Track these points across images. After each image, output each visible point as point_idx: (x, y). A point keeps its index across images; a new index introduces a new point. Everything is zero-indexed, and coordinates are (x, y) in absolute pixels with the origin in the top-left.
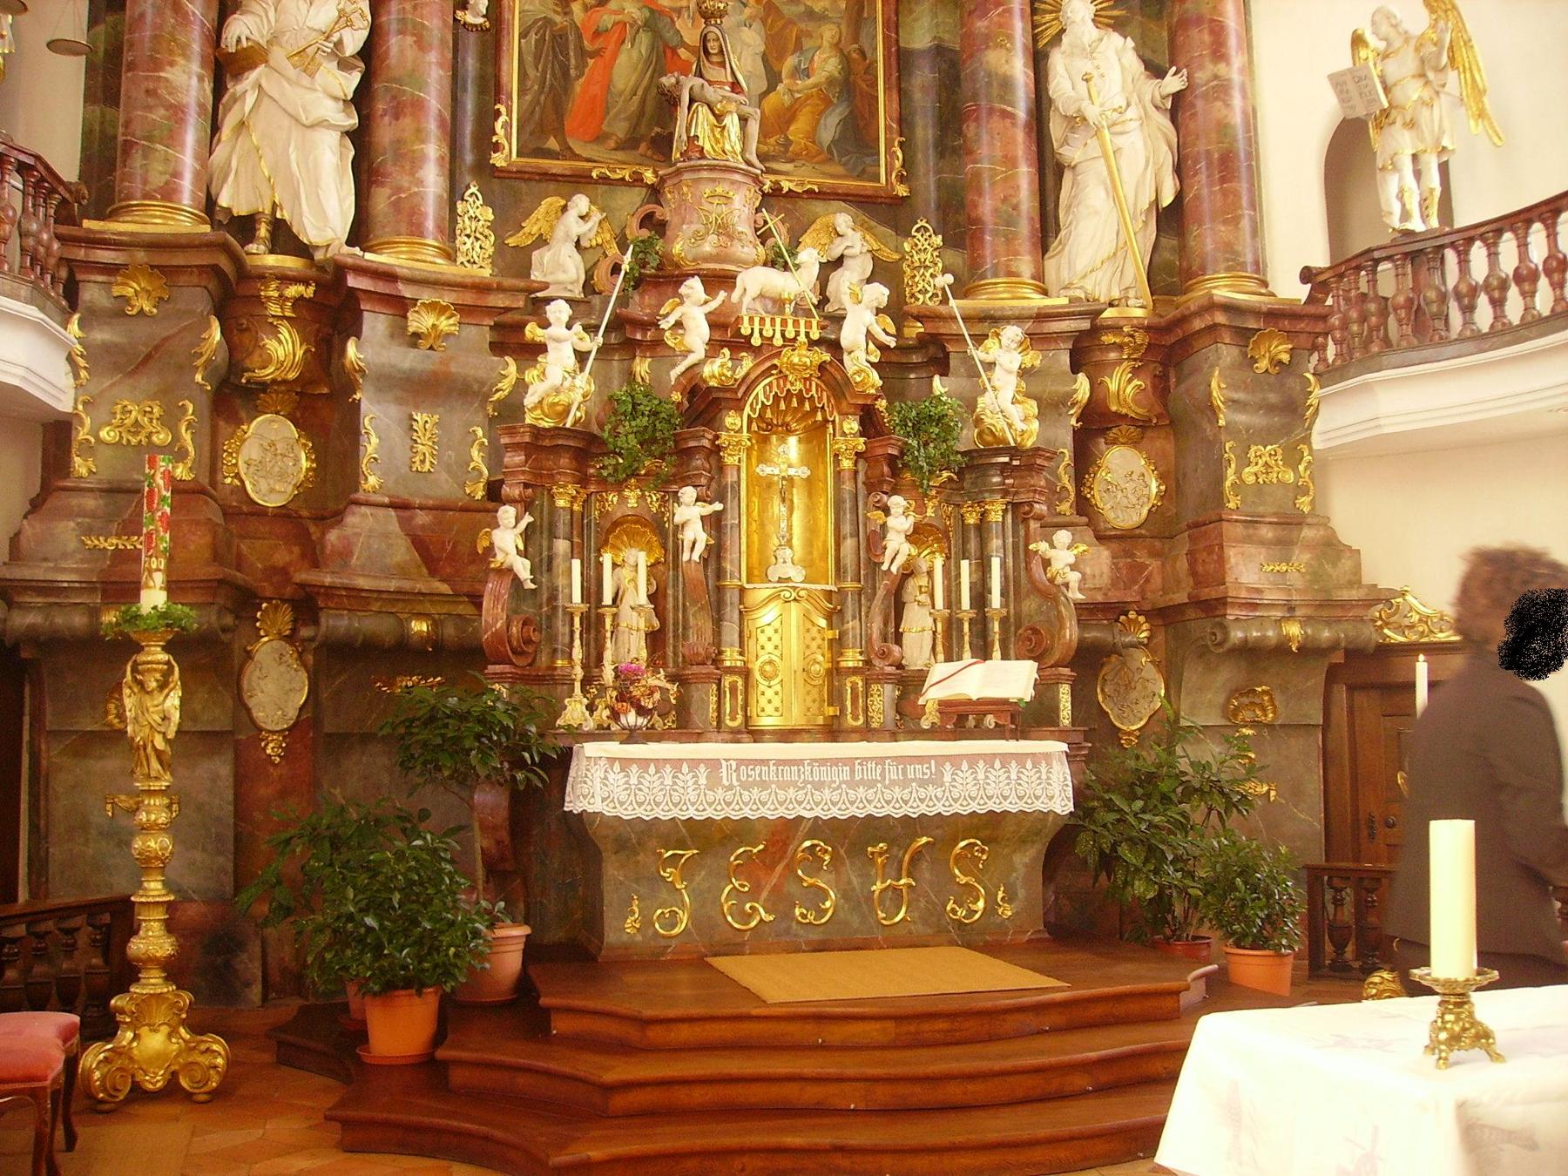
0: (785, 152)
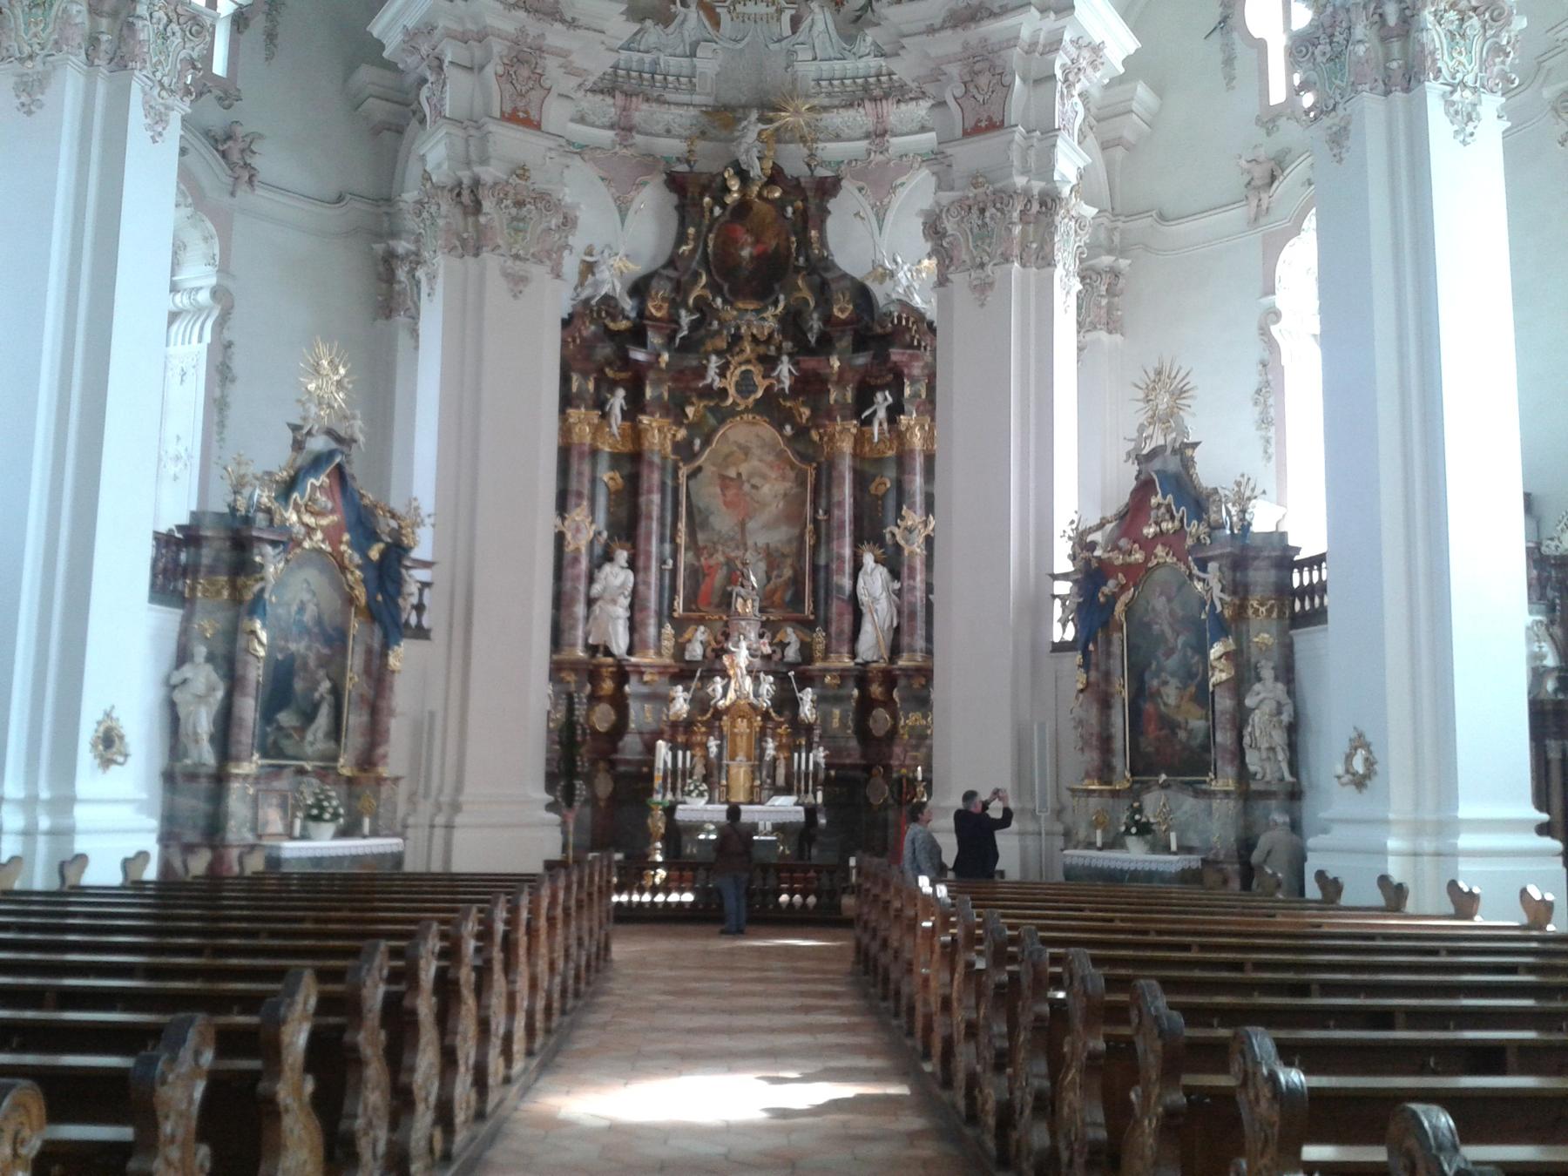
0: (773, 605)
